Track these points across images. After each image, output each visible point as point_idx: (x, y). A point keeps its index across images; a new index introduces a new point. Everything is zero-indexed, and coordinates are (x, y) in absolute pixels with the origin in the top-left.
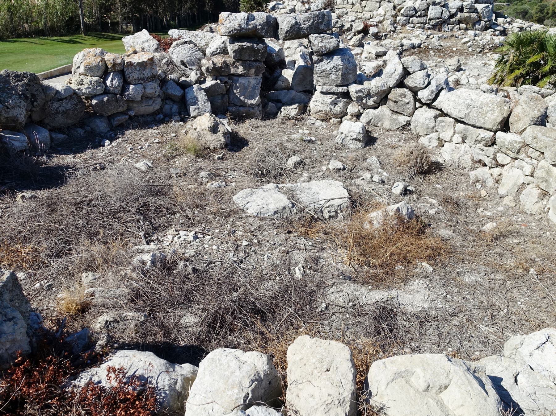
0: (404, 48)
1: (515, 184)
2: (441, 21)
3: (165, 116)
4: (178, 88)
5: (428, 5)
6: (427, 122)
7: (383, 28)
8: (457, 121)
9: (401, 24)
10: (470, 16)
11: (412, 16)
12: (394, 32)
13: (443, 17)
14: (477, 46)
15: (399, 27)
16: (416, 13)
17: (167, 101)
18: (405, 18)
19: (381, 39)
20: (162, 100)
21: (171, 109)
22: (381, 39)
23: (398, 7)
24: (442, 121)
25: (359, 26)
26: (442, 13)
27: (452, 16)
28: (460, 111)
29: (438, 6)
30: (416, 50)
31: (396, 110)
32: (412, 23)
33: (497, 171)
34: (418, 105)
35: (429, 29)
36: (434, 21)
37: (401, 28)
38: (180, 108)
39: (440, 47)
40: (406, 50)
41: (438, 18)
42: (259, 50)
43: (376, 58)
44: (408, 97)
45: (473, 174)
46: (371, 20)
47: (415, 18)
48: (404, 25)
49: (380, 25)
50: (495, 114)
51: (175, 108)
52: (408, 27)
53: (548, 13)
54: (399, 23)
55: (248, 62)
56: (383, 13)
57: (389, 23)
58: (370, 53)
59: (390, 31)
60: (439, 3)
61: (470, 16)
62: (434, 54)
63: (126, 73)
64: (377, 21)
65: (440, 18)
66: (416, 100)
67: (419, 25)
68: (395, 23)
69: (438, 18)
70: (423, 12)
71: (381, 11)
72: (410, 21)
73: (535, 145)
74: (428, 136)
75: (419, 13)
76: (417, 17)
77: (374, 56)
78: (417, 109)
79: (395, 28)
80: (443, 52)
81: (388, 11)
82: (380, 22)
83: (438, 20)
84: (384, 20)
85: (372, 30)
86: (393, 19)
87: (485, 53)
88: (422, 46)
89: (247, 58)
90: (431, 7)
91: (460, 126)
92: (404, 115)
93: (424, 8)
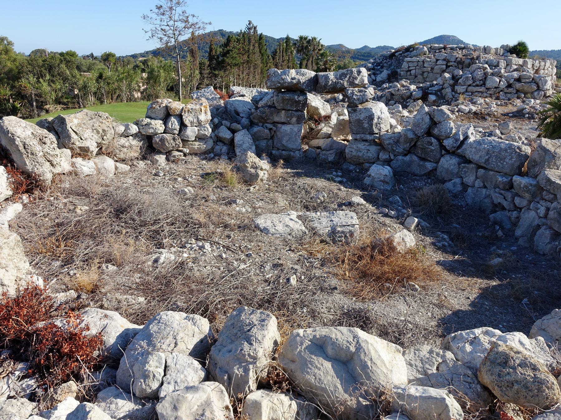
1: (531, 225)
3: (215, 155)
4: (229, 132)
6: (452, 167)
8: (479, 167)
17: (218, 143)
20: (214, 142)
21: (221, 150)
24: (464, 167)
28: (480, 157)
31: (423, 156)
33: (515, 214)
34: (443, 152)
38: (229, 149)
42: (300, 101)
44: (434, 144)
45: (492, 216)
50: (513, 160)
51: (225, 149)
55: (291, 112)
56: (441, 83)
63: (184, 117)
66: (442, 147)
73: (549, 187)
74: (453, 181)
78: (442, 156)
84: (443, 89)
89: (289, 108)
91: (481, 171)
92: (431, 161)
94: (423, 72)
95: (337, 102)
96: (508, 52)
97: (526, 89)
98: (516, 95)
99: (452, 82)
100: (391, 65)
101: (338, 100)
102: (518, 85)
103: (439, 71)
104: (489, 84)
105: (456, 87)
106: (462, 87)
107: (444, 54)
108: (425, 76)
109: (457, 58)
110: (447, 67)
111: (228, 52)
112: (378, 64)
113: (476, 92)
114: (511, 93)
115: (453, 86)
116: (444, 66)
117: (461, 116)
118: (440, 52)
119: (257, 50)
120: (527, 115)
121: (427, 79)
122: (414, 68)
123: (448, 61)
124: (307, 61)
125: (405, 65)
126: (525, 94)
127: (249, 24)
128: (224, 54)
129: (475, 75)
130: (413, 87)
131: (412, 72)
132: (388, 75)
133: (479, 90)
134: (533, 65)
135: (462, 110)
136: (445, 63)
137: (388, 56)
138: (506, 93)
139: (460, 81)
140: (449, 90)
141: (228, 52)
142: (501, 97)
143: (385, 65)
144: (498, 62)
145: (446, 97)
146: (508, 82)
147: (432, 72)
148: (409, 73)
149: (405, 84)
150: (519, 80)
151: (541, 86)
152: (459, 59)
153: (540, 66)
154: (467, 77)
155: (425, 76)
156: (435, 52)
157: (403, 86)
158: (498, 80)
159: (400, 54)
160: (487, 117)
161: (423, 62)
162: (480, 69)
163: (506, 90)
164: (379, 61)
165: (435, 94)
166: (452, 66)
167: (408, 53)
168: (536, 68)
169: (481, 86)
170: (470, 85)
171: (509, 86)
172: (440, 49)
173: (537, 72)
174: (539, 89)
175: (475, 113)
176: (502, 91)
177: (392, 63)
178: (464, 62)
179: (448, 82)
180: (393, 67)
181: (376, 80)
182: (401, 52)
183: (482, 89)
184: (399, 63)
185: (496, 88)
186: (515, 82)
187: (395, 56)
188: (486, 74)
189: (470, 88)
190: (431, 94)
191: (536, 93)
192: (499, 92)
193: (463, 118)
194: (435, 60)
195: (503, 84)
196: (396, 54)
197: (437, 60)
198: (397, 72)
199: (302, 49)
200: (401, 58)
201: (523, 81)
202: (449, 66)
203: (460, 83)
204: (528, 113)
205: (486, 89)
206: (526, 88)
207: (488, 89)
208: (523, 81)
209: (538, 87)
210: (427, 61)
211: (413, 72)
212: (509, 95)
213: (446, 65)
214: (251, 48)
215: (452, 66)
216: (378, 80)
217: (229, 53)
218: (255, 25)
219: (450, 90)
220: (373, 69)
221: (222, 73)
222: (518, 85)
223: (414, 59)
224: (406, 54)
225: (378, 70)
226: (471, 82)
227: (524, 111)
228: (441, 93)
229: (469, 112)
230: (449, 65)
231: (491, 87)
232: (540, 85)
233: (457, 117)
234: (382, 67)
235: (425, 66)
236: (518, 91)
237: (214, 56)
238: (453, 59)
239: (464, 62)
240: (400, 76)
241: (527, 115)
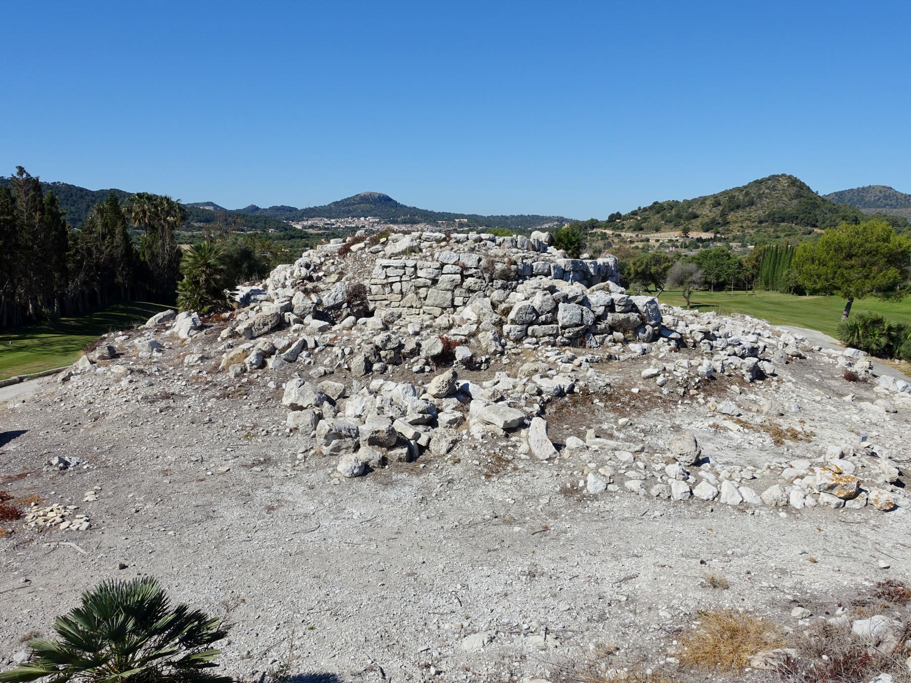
0: (546, 397)
2: (582, 330)
5: (557, 302)
7: (479, 346)
9: (512, 338)
10: (628, 318)
11: (532, 323)
12: (502, 353)
13: (585, 322)
14: (675, 384)
15: (510, 344)
16: (537, 318)
18: (519, 328)
19: (479, 369)
22: (479, 369)
23: (503, 306)
25: (433, 346)
26: (582, 315)
27: (599, 319)
29: (573, 304)
30: (566, 399)
32: (533, 336)
35: (564, 344)
36: (571, 330)
37: (515, 345)
39: (608, 389)
40: (549, 401)
41: (577, 325)
43: (507, 436)
46: (453, 331)
47: (536, 327)
48: (518, 340)
49: (472, 340)
52: (527, 344)
53: (629, 274)
54: (508, 336)
56: (474, 318)
57: (491, 337)
58: (488, 423)
59: (495, 353)
60: (574, 298)
61: (628, 318)
62: (602, 404)
64: (466, 333)
65: (581, 325)
67: (546, 339)
68: (501, 336)
69: (577, 325)
70: (549, 315)
71: (468, 313)
72: (530, 332)
75: (543, 318)
76: (539, 325)
77: (501, 433)
79: (503, 346)
80: (617, 399)
81: (484, 314)
82: (473, 335)
83: (577, 329)
85: (461, 353)
86: (495, 329)
87: (692, 397)
88: (576, 390)
90: (561, 305)
93: (549, 308)
116: (458, 277)
121: (427, 302)
122: (398, 279)
123: (464, 268)
131: (395, 286)
136: (457, 268)
148: (387, 289)
155: (422, 296)
161: (415, 267)
166: (472, 276)
167: (378, 247)
177: (347, 266)
184: (364, 266)
187: (350, 251)
196: (354, 248)
197: (443, 265)
211: (397, 287)
213: (461, 273)
224: (374, 248)
230: (465, 273)
240: (370, 293)
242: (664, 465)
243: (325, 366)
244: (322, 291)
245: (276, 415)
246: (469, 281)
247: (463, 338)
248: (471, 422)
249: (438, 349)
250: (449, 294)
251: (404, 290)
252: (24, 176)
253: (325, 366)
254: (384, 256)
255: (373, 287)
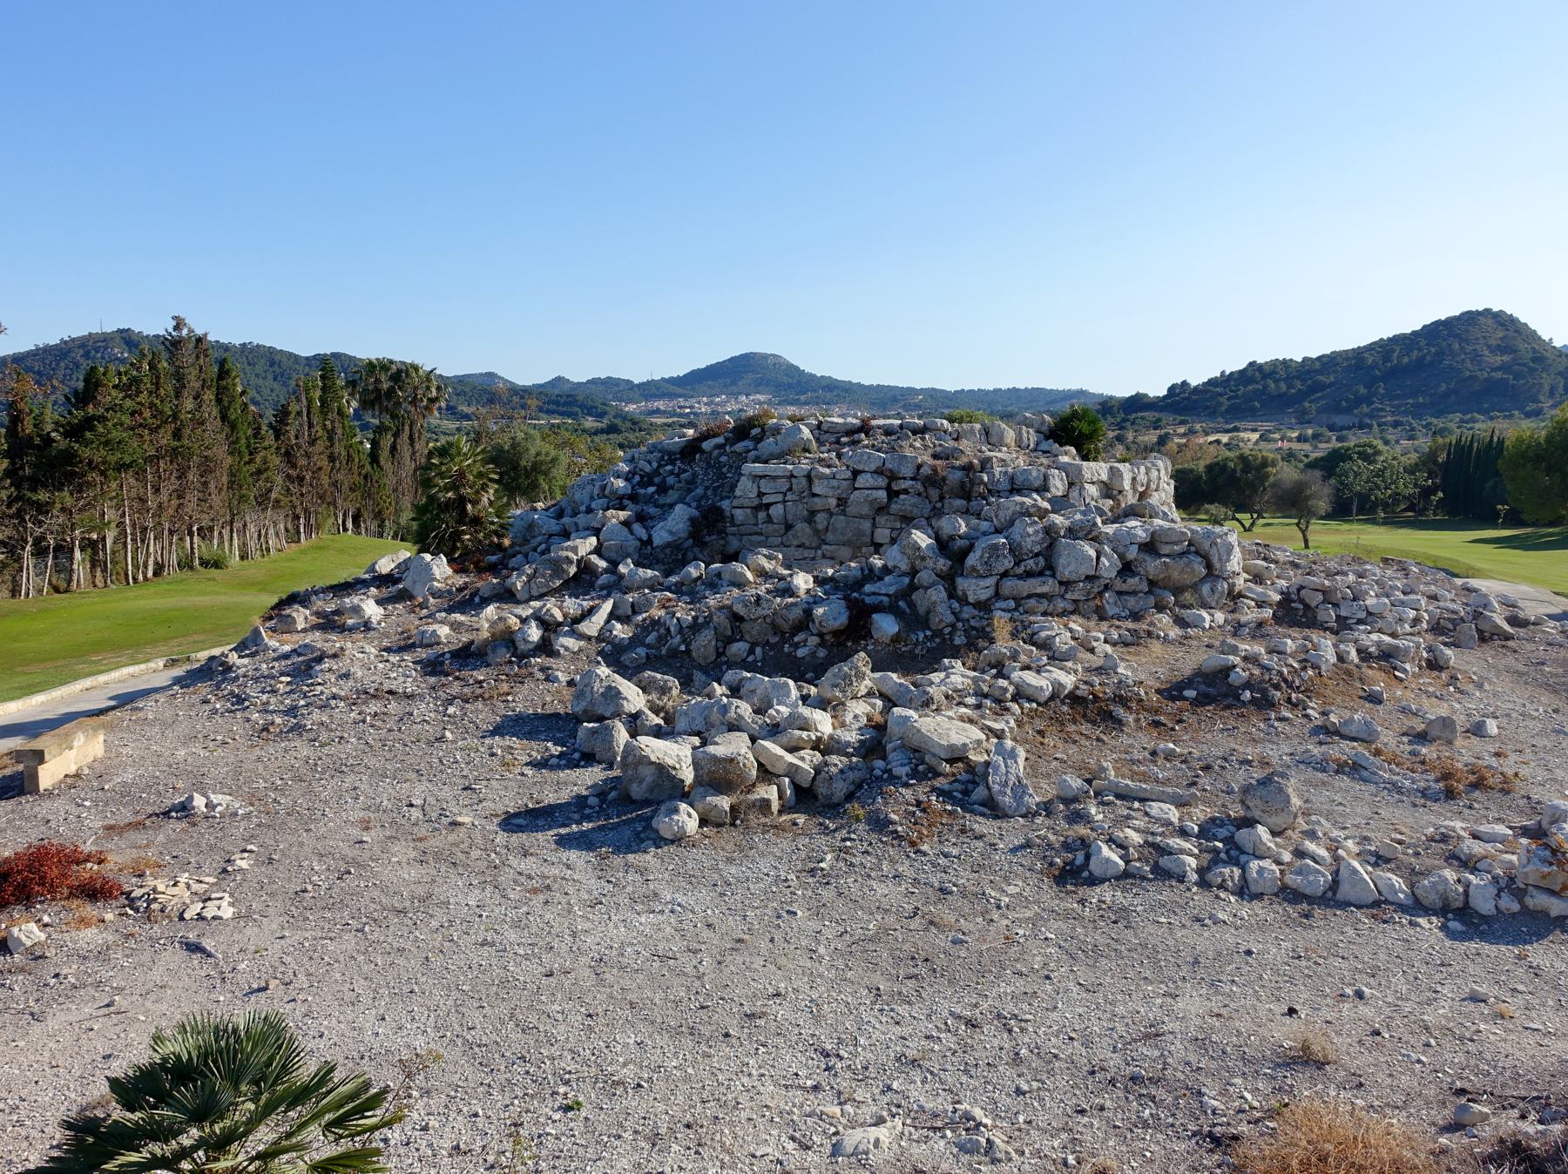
46: (868, 588)
56: (904, 567)
64: (892, 590)
84: (913, 587)
94: (813, 513)
95: (522, 656)
96: (1047, 438)
97: (1176, 574)
98: (1151, 600)
99: (943, 564)
100: (692, 482)
101: (522, 646)
102: (1153, 566)
103: (866, 510)
104: (1067, 567)
105: (962, 584)
106: (982, 583)
107: (870, 454)
108: (820, 527)
109: (919, 467)
110: (893, 494)
111: (88, 423)
112: (647, 480)
113: (1029, 596)
114: (1134, 593)
115: (949, 579)
116: (883, 494)
117: (1032, 715)
118: (855, 443)
119: (211, 410)
120: (1247, 695)
121: (830, 537)
122: (780, 498)
123: (893, 477)
124: (396, 435)
125: (746, 489)
126: (1178, 591)
127: (177, 328)
128: (74, 432)
129: (1018, 538)
130: (803, 581)
131: (772, 511)
132: (692, 520)
133: (1039, 590)
134: (1134, 479)
135: (1030, 692)
137: (676, 449)
138: (1119, 593)
139: (972, 560)
140: (938, 594)
141: (88, 423)
142: (1111, 610)
143: (671, 480)
144: (1046, 478)
145: (934, 622)
146: (1121, 557)
147: (844, 513)
148: (762, 515)
149: (769, 566)
150: (1150, 547)
151: (1217, 566)
152: (926, 471)
153: (1149, 481)
154: (995, 547)
156: (838, 442)
157: (763, 574)
158: (1093, 553)
159: (718, 447)
160: (1120, 712)
161: (809, 477)
162: (1030, 515)
163: (1119, 585)
164: (648, 469)
165: (892, 609)
167: (747, 443)
168: (1141, 489)
169: (1041, 574)
170: (1005, 574)
171: (1127, 569)
172: (851, 432)
173: (1143, 496)
174: (1212, 573)
175: (1074, 699)
176: (1106, 587)
177: (695, 475)
178: (944, 479)
179: (930, 563)
180: (700, 491)
181: (650, 541)
182: (720, 440)
183: (1048, 586)
184: (722, 476)
185: (1089, 578)
186: (1141, 556)
187: (702, 452)
188: (1050, 531)
189: (1009, 585)
190: (878, 608)
191: (1206, 589)
192: (1101, 594)
193: (1040, 724)
194: (849, 474)
195: (1110, 566)
196: (706, 445)
198: (720, 511)
199: (378, 398)
200: (723, 459)
201: (1165, 550)
202: (897, 493)
203: (974, 569)
204: (1248, 685)
205: (1061, 583)
206: (1178, 572)
207: (1066, 584)
208: (1165, 550)
209: (1209, 566)
210: (823, 477)
212: (1131, 601)
213: (888, 488)
214: (189, 404)
215: (906, 491)
216: (657, 541)
217: (92, 428)
218: (199, 332)
219: (944, 595)
220: (633, 497)
221: (66, 497)
222: (1153, 566)
223: (773, 468)
224: (739, 447)
225: (649, 500)
226: (1007, 563)
227: (1233, 678)
228: (911, 605)
229: (1053, 697)
231: (1074, 577)
232: (1215, 561)
233: (1020, 724)
234: (663, 489)
235: (817, 489)
236: (1152, 583)
237: (30, 438)
238: (907, 471)
239: (944, 479)
241: (1247, 695)
242: (1232, 829)
243: (648, 646)
244: (652, 518)
245: (559, 730)
246: (905, 503)
247: (886, 599)
248: (889, 747)
249: (842, 620)
250: (866, 525)
251: (790, 517)
252: (185, 332)
253: (648, 646)
254: (757, 460)
255: (738, 512)
